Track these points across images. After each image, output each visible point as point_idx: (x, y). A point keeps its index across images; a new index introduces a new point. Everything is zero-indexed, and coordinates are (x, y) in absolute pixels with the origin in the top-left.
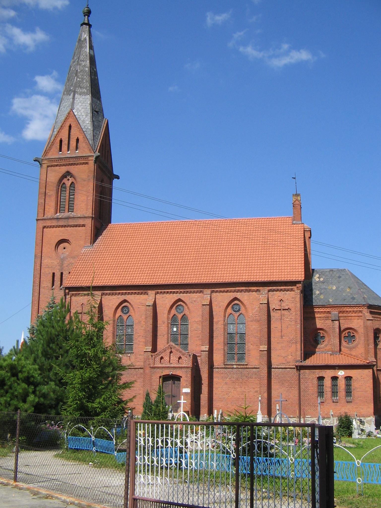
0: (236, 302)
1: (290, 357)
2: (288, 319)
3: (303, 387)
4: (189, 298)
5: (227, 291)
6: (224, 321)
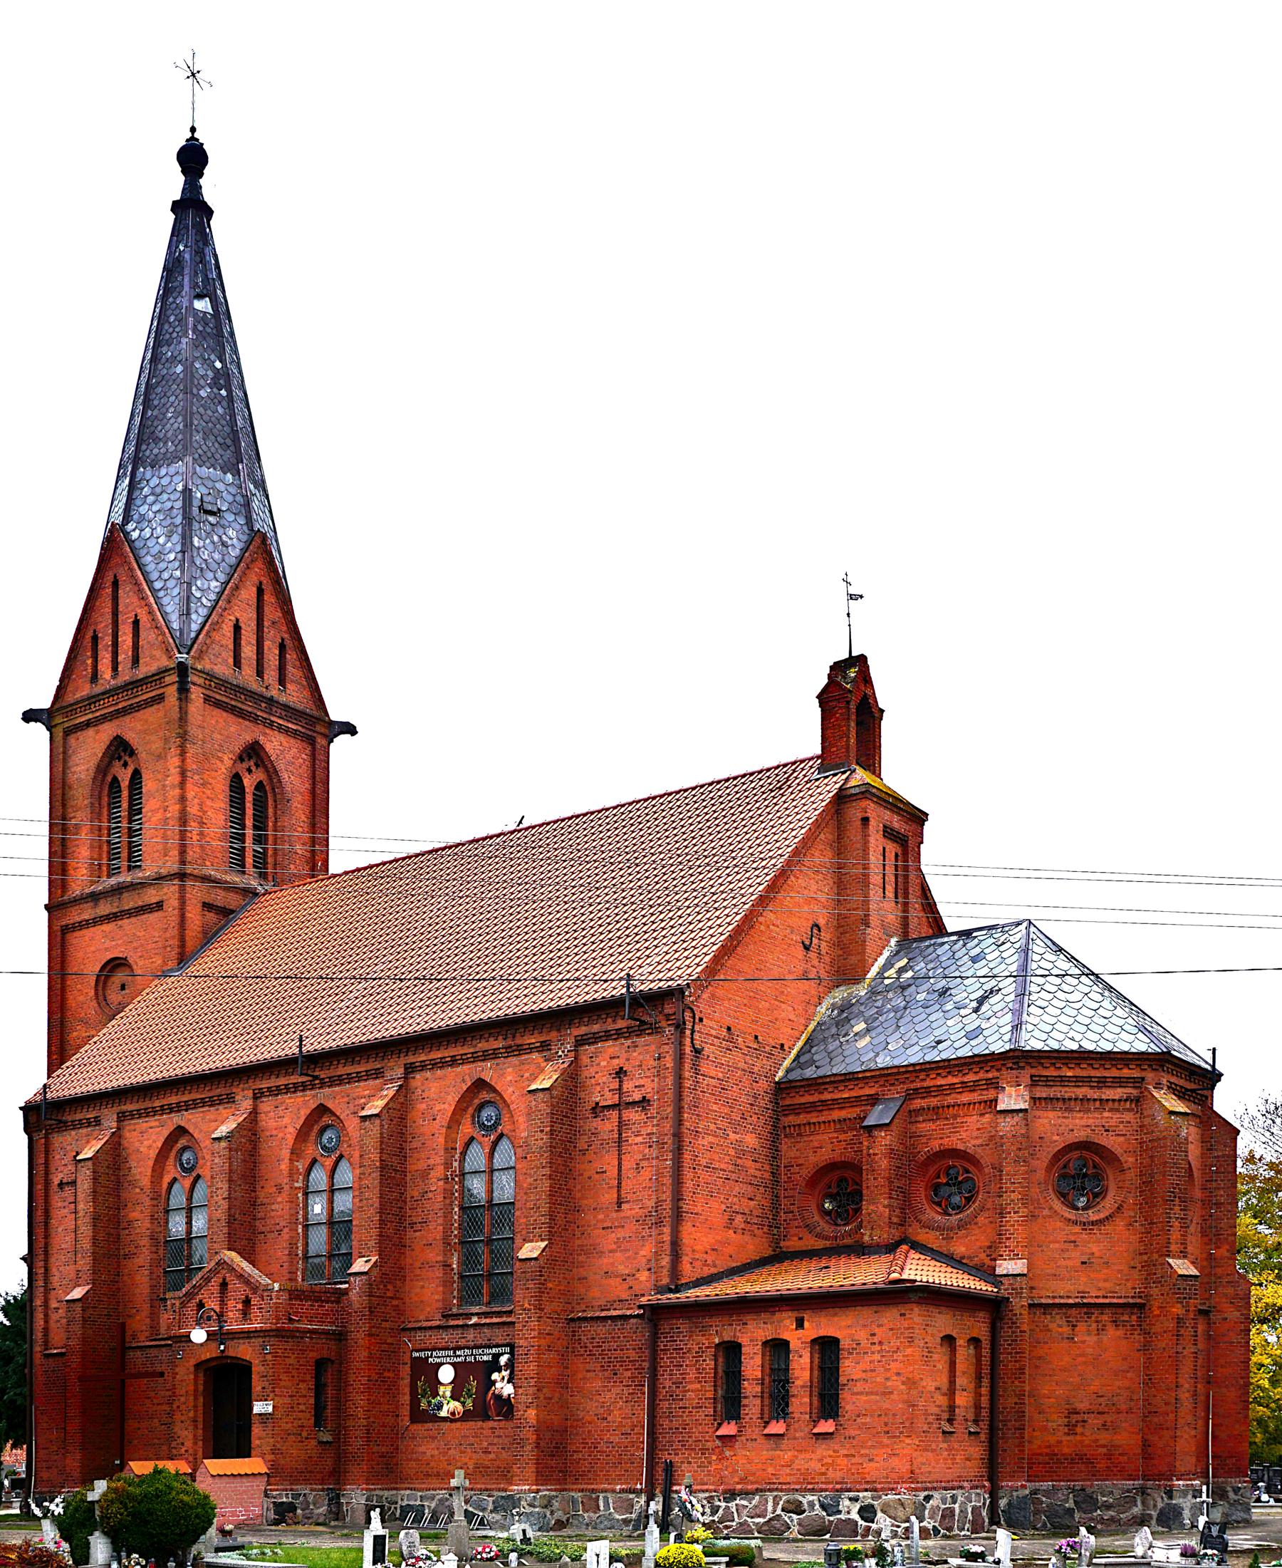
0: (485, 1096)
1: (643, 1276)
2: (639, 1139)
3: (668, 1383)
4: (346, 1099)
5: (454, 1062)
6: (448, 1165)
